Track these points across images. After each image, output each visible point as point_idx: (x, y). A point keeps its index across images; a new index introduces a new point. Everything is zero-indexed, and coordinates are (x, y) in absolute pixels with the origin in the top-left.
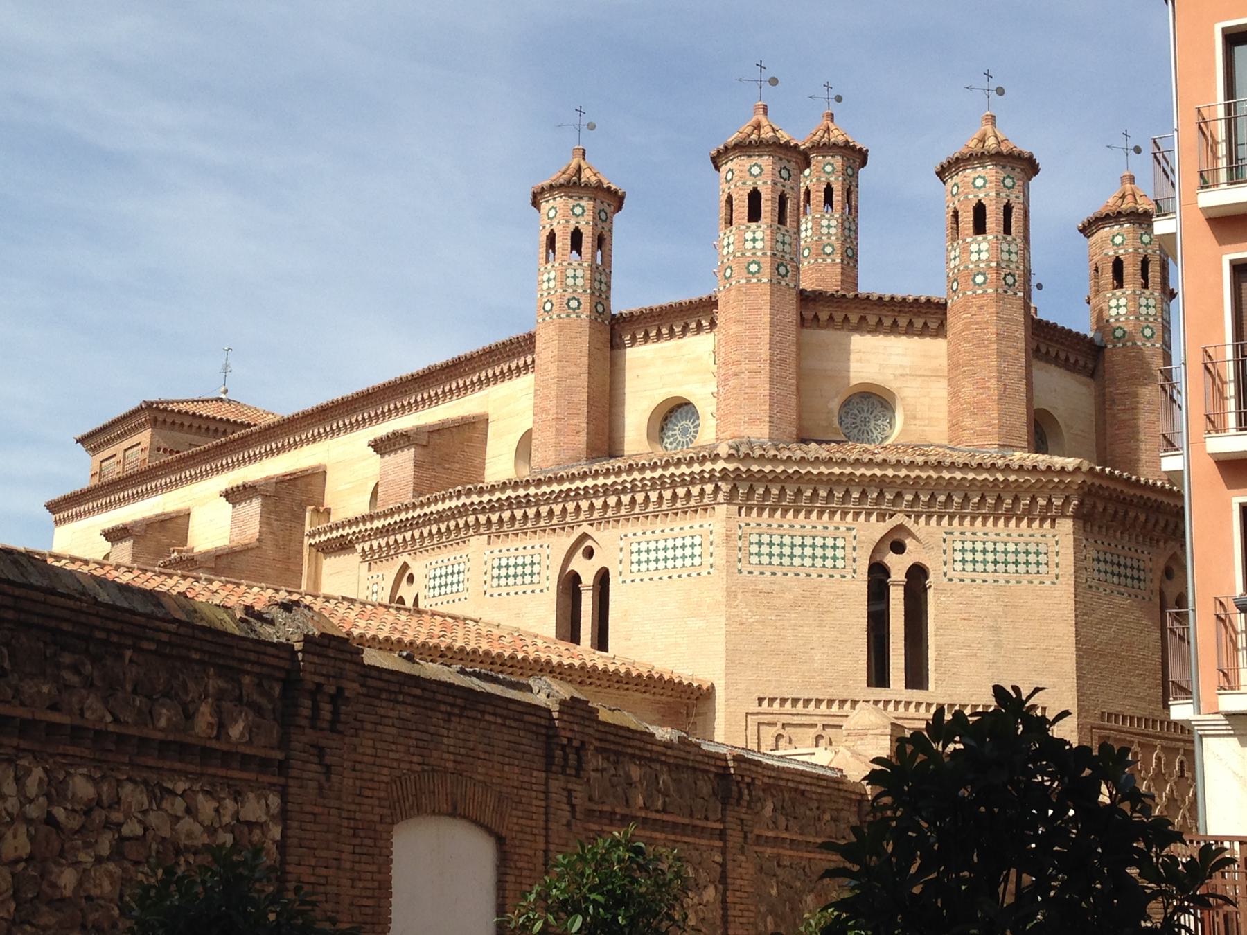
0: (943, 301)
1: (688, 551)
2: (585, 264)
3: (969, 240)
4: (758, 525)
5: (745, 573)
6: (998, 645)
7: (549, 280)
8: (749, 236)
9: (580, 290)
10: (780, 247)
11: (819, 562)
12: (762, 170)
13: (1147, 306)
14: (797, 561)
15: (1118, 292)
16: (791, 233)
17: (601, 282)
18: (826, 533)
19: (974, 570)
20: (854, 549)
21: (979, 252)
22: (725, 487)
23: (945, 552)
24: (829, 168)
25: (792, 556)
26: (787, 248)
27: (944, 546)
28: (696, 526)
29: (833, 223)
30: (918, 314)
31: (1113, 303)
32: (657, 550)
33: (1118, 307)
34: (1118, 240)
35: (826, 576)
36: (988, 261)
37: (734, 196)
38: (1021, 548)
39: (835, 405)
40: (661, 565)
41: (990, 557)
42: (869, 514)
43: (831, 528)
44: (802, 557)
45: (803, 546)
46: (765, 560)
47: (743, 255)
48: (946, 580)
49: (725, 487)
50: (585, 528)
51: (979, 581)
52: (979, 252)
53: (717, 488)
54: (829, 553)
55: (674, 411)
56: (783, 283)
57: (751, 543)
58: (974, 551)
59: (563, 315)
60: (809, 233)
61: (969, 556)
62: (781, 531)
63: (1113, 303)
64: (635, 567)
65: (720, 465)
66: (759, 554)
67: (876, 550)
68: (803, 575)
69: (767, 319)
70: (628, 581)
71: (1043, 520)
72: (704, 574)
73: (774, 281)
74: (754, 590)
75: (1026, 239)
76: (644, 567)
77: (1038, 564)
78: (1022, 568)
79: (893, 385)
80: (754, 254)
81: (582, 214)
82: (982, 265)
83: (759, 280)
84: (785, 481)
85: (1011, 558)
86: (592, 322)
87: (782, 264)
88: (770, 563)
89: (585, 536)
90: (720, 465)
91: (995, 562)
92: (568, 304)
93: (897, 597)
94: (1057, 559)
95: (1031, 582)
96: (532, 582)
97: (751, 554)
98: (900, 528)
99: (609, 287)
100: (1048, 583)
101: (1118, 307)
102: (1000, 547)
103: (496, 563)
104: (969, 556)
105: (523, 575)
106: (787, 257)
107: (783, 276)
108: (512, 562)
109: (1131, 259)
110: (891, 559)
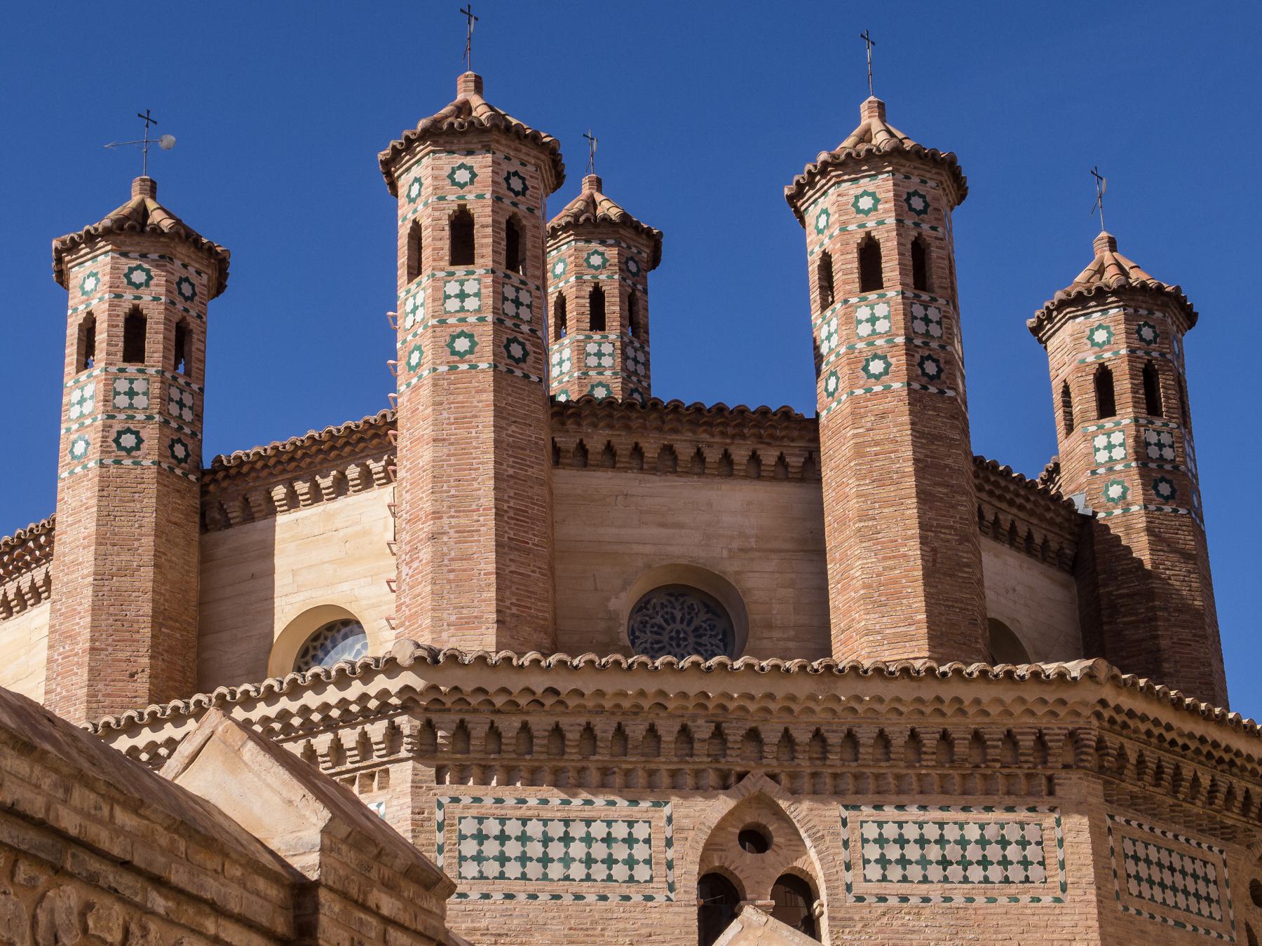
0: (809, 415)
2: (152, 371)
3: (853, 300)
4: (477, 800)
8: (452, 288)
9: (140, 417)
10: (510, 308)
11: (599, 871)
12: (474, 175)
14: (555, 870)
15: (1108, 423)
16: (531, 286)
17: (181, 404)
19: (905, 879)
20: (669, 843)
21: (873, 320)
23: (846, 844)
24: (596, 260)
25: (545, 860)
26: (525, 313)
27: (845, 833)
29: (607, 348)
31: (1101, 441)
33: (1110, 447)
34: (1101, 336)
35: (614, 899)
36: (890, 336)
37: (425, 222)
39: (623, 603)
41: (934, 852)
45: (567, 839)
46: (492, 868)
47: (442, 322)
48: (850, 899)
49: (406, 723)
51: (914, 901)
52: (873, 320)
53: (394, 733)
54: (621, 852)
56: (518, 373)
57: (462, 837)
58: (902, 841)
59: (108, 461)
60: (566, 366)
61: (893, 853)
62: (523, 812)
63: (1101, 441)
65: (394, 685)
66: (479, 858)
67: (710, 847)
68: (568, 899)
69: (488, 435)
73: (502, 368)
75: (952, 300)
77: (1025, 863)
78: (995, 872)
79: (730, 568)
80: (463, 320)
81: (147, 284)
82: (880, 342)
83: (473, 367)
85: (973, 853)
86: (164, 475)
87: (515, 340)
88: (502, 876)
91: (945, 863)
92: (117, 441)
94: (1060, 854)
95: (1017, 900)
97: (462, 859)
99: (199, 417)
100: (1047, 900)
101: (1110, 447)
104: (893, 853)
106: (525, 328)
107: (518, 361)
109: (1125, 366)
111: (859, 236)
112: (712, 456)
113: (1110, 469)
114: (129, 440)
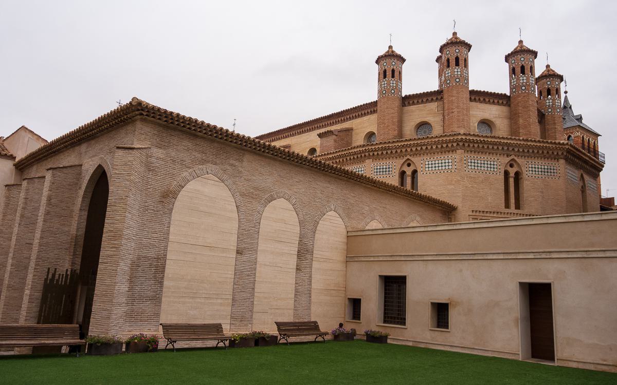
1: (447, 164)
5: (467, 171)
6: (543, 197)
7: (384, 84)
13: (558, 103)
14: (482, 168)
18: (491, 160)
21: (523, 80)
22: (461, 144)
28: (450, 156)
30: (501, 99)
32: (435, 164)
33: (549, 102)
34: (549, 83)
36: (526, 83)
38: (549, 167)
39: (476, 125)
40: (437, 168)
41: (540, 170)
42: (504, 155)
43: (493, 159)
44: (484, 167)
46: (473, 167)
50: (408, 157)
52: (523, 80)
54: (492, 166)
55: (423, 125)
58: (535, 168)
61: (534, 169)
62: (477, 159)
64: (427, 169)
65: (460, 137)
66: (471, 166)
70: (425, 173)
71: (555, 159)
72: (453, 171)
74: (470, 177)
76: (430, 169)
77: (554, 173)
79: (493, 120)
84: (479, 143)
85: (546, 170)
89: (408, 159)
90: (460, 137)
91: (541, 172)
93: (512, 181)
96: (389, 174)
98: (513, 160)
101: (549, 102)
102: (543, 167)
103: (376, 168)
104: (534, 169)
105: (386, 171)
108: (381, 167)
110: (510, 169)
111: (521, 65)
112: (491, 101)
113: (549, 106)
114: (393, 91)
